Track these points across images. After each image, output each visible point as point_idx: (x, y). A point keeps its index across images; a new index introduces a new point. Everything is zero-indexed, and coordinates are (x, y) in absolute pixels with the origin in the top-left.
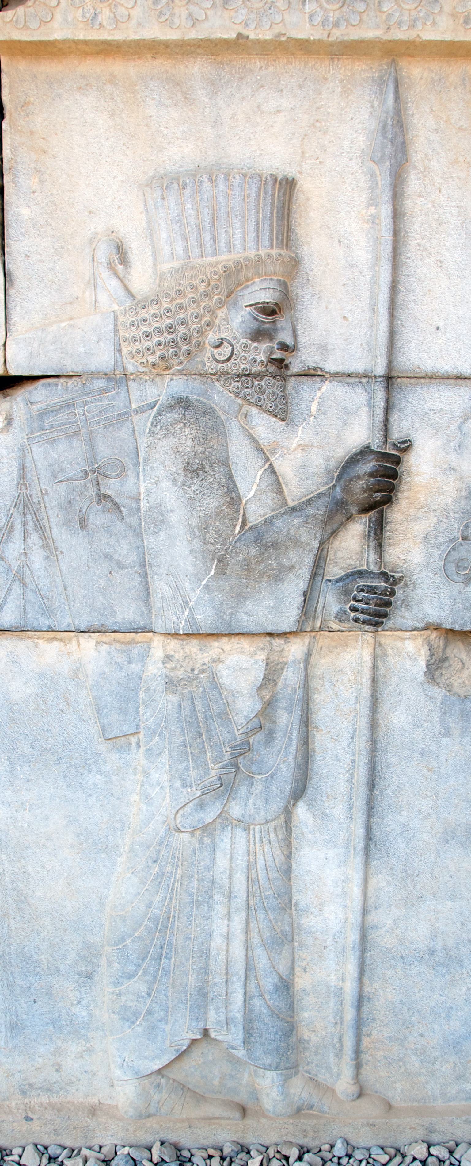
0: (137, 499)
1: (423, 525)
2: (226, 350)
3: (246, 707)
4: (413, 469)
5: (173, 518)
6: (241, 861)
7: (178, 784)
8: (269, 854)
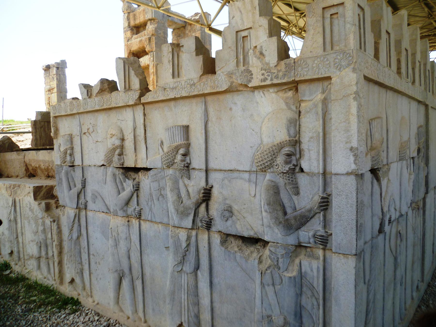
3: (184, 245)
4: (214, 192)
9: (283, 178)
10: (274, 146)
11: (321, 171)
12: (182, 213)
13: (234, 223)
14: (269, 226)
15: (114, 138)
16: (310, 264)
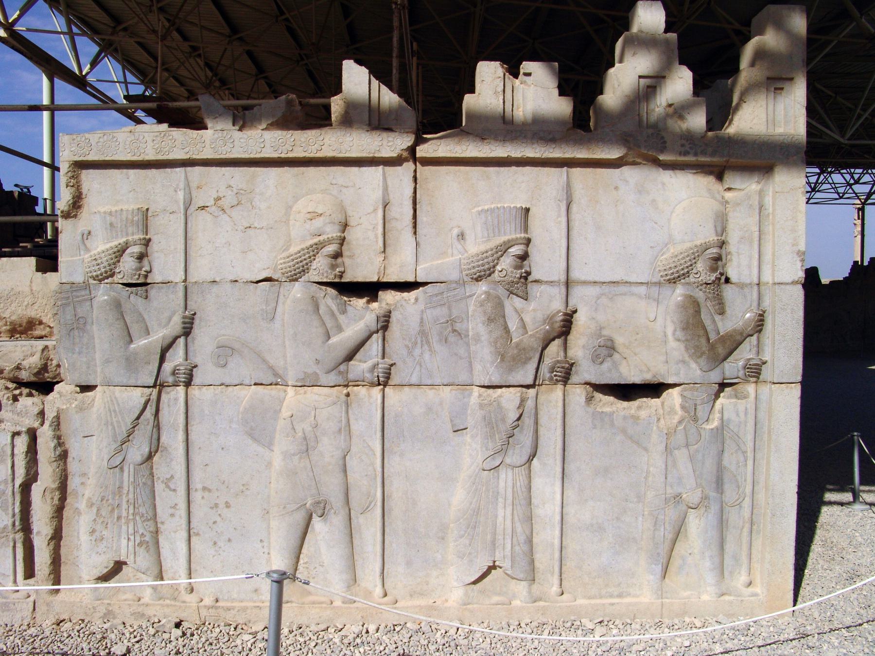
0: (467, 331)
1: (582, 341)
2: (504, 273)
3: (513, 415)
5: (483, 338)
6: (510, 484)
7: (484, 449)
8: (521, 481)
9: (705, 292)
10: (696, 246)
11: (756, 281)
12: (514, 359)
13: (616, 365)
14: (684, 362)
15: (318, 223)
16: (735, 405)
